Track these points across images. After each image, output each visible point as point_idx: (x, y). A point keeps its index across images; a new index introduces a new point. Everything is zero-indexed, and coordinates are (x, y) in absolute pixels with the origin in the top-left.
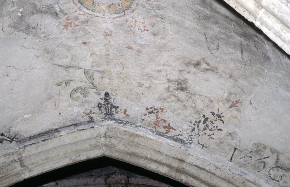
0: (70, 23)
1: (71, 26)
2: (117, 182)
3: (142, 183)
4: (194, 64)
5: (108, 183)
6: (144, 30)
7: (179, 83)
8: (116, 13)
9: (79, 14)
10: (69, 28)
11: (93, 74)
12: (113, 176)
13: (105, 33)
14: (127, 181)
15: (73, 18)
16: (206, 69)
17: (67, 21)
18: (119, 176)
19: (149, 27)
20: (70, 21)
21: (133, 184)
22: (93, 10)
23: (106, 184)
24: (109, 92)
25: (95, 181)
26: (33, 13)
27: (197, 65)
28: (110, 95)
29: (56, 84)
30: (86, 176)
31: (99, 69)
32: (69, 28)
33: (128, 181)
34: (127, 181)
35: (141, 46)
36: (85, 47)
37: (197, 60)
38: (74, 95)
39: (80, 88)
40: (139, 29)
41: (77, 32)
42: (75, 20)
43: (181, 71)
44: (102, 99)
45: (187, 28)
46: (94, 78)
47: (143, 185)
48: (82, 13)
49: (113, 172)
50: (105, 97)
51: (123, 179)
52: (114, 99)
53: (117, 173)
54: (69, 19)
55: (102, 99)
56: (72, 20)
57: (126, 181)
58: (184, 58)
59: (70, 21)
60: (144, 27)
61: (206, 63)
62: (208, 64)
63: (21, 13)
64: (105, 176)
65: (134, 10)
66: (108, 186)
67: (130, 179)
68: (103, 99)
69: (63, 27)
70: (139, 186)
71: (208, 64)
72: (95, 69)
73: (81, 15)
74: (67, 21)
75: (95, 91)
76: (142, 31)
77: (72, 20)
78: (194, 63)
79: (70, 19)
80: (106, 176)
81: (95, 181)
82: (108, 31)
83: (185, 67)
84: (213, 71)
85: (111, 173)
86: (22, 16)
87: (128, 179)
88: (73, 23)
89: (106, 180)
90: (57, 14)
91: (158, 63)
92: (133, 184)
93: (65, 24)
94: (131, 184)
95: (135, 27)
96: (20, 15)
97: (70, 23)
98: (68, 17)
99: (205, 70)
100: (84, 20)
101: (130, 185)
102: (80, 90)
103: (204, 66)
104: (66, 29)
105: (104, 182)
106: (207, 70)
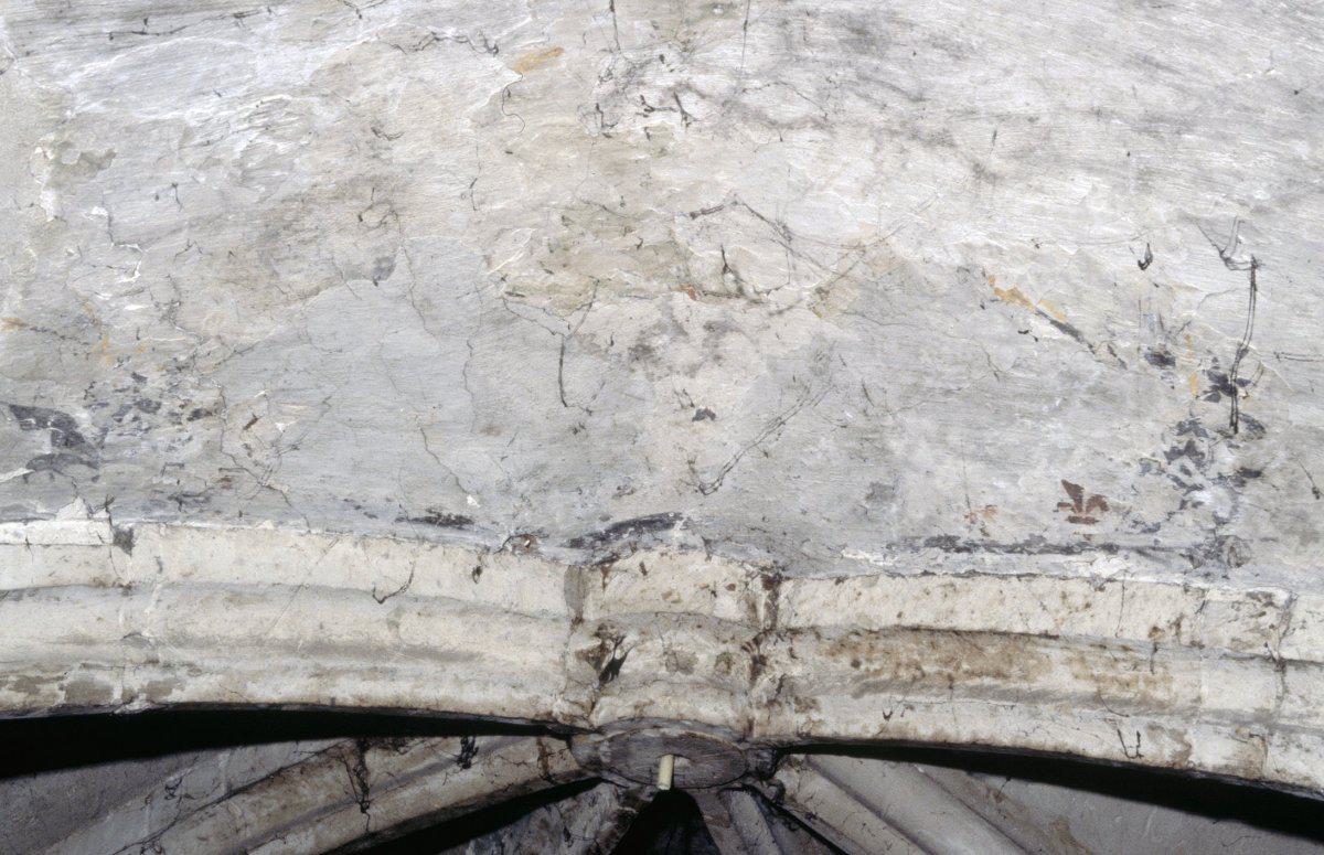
2: (678, 608)
3: (899, 615)
5: (592, 615)
12: (641, 556)
14: (762, 612)
18: (697, 563)
21: (818, 636)
23: (578, 621)
25: (478, 571)
30: (399, 520)
33: (773, 610)
34: (762, 612)
47: (905, 629)
49: (645, 512)
51: (732, 587)
53: (676, 533)
57: (753, 608)
64: (576, 543)
66: (597, 642)
67: (786, 588)
70: (865, 646)
80: (577, 556)
81: (478, 571)
85: (619, 528)
87: (776, 596)
89: (576, 587)
92: (818, 636)
94: (795, 632)
101: (783, 646)
105: (556, 603)
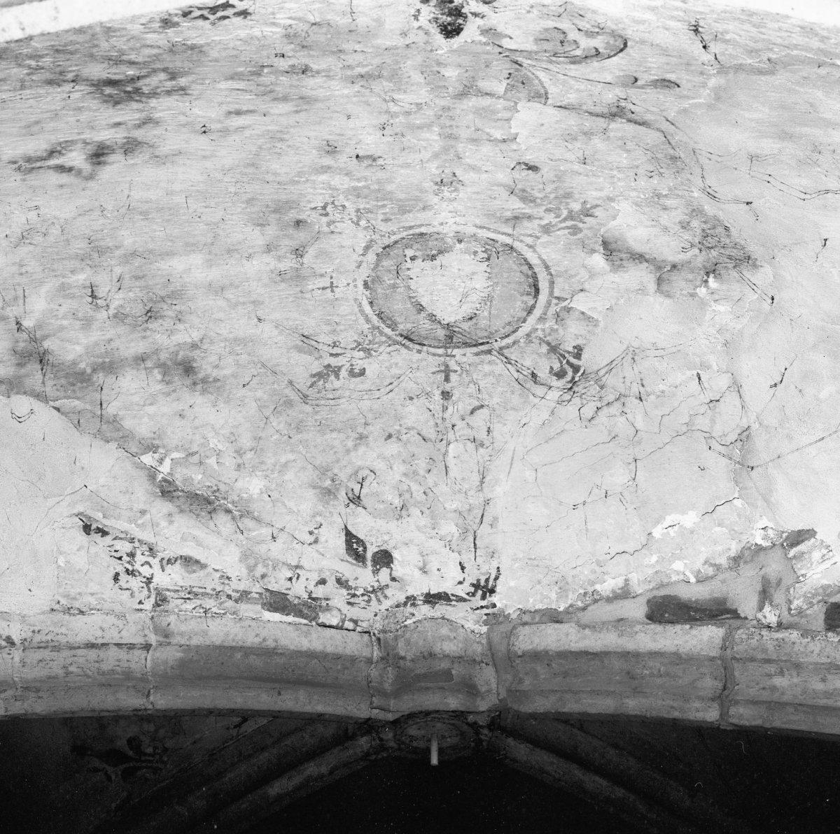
0: (571, 216)
1: (571, 212)
4: (113, 151)
6: (324, 208)
7: (137, 91)
8: (422, 234)
9: (538, 238)
10: (576, 207)
11: (510, 88)
13: (456, 190)
15: (559, 230)
16: (60, 152)
17: (581, 225)
19: (313, 217)
20: (569, 223)
22: (491, 242)
24: (439, 38)
26: (674, 266)
27: (99, 155)
28: (434, 31)
29: (679, 86)
31: (487, 101)
32: (576, 207)
35: (326, 169)
36: (529, 158)
37: (108, 168)
38: (608, 43)
39: (575, 61)
40: (344, 207)
41: (552, 196)
42: (553, 226)
43: (147, 122)
44: (475, 15)
45: (191, 247)
46: (508, 78)
48: (529, 240)
50: (460, 21)
52: (416, 17)
54: (571, 230)
55: (475, 15)
56: (563, 225)
58: (159, 160)
59: (569, 223)
60: (327, 215)
61: (70, 169)
62: (61, 169)
63: (706, 281)
65: (367, 248)
68: (469, 15)
69: (597, 212)
71: (61, 169)
72: (501, 104)
73: (531, 236)
74: (581, 225)
75: (506, 43)
76: (333, 203)
77: (563, 225)
78: (111, 158)
79: (568, 228)
82: (447, 194)
83: (139, 134)
84: (29, 160)
86: (708, 274)
88: (560, 219)
90: (605, 244)
91: (247, 133)
93: (587, 219)
95: (358, 210)
96: (711, 280)
97: (571, 216)
98: (574, 234)
99: (59, 148)
100: (526, 223)
102: (578, 52)
103: (76, 158)
104: (588, 206)
106: (52, 153)
